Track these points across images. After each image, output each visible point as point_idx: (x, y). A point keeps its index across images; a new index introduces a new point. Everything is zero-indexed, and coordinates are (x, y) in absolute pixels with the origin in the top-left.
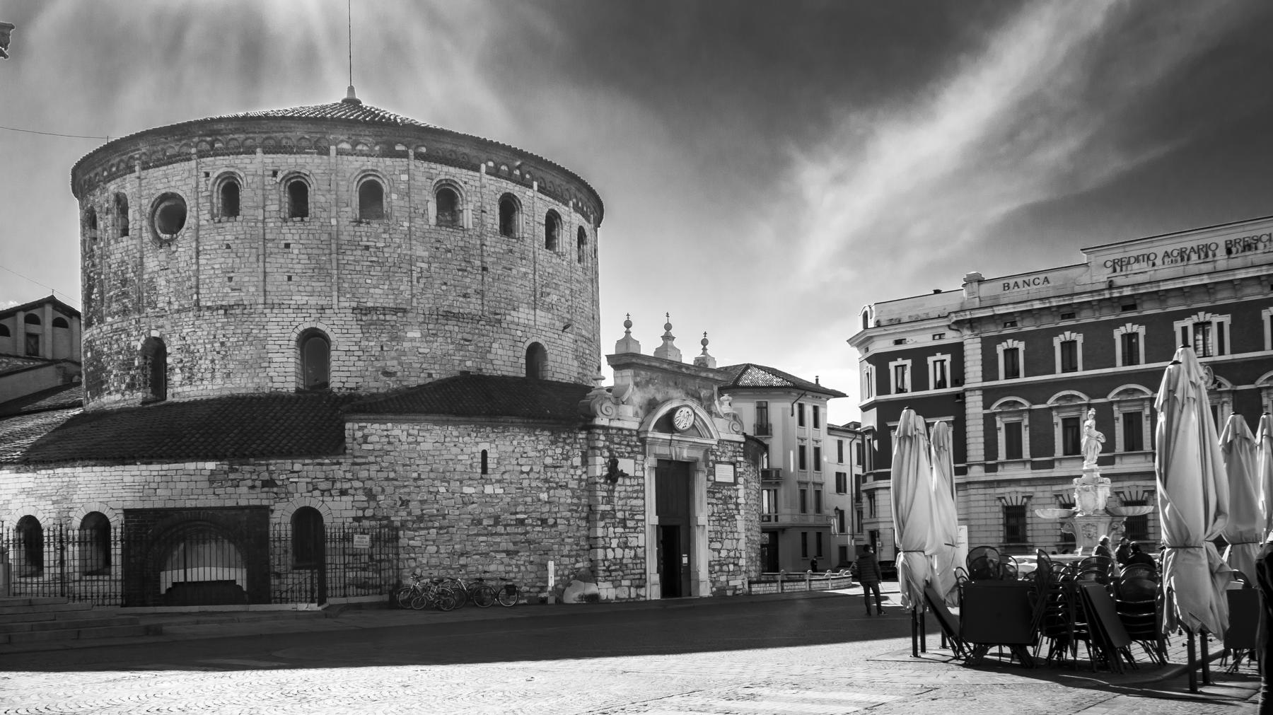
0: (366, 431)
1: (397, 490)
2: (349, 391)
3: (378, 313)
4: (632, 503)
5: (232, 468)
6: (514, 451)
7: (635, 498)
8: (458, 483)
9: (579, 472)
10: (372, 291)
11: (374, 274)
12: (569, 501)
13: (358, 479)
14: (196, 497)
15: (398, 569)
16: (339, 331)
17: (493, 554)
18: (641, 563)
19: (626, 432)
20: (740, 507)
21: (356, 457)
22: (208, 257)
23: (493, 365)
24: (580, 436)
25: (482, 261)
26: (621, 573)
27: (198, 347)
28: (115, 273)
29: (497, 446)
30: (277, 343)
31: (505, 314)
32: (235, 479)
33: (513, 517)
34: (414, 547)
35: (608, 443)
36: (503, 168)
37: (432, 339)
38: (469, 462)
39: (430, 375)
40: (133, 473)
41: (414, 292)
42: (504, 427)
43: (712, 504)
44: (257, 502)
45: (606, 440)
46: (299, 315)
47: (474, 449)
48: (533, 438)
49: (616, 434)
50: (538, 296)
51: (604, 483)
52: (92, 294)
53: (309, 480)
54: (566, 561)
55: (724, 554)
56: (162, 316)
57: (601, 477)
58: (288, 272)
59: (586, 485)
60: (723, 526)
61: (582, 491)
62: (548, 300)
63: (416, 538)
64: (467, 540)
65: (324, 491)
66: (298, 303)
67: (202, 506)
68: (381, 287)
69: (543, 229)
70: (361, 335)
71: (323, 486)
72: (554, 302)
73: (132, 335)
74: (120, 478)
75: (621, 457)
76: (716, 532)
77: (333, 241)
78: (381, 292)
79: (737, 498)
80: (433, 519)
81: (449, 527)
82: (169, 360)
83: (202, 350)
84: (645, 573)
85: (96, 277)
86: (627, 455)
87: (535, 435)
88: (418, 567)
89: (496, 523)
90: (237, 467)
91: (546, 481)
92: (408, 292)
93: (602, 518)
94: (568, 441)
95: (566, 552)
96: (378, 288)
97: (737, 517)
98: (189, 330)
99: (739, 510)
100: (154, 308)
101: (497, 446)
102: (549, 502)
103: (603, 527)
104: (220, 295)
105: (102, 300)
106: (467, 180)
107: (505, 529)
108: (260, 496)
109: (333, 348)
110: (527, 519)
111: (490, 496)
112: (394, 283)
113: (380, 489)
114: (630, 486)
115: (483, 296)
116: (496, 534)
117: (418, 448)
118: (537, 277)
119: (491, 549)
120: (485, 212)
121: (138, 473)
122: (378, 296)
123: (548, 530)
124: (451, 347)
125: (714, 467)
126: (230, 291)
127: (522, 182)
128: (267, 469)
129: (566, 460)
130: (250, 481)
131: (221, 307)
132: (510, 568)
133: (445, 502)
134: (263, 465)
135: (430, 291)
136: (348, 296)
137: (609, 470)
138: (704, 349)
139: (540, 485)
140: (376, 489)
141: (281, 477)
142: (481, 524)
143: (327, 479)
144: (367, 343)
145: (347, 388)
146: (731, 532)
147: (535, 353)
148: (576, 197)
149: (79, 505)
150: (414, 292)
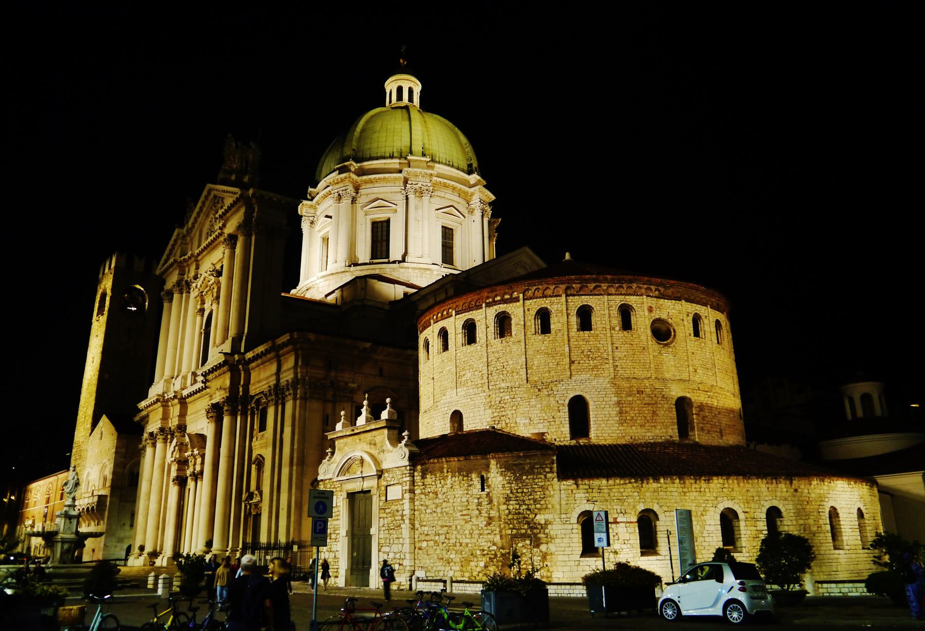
20: (405, 518)
43: (384, 518)
97: (402, 526)
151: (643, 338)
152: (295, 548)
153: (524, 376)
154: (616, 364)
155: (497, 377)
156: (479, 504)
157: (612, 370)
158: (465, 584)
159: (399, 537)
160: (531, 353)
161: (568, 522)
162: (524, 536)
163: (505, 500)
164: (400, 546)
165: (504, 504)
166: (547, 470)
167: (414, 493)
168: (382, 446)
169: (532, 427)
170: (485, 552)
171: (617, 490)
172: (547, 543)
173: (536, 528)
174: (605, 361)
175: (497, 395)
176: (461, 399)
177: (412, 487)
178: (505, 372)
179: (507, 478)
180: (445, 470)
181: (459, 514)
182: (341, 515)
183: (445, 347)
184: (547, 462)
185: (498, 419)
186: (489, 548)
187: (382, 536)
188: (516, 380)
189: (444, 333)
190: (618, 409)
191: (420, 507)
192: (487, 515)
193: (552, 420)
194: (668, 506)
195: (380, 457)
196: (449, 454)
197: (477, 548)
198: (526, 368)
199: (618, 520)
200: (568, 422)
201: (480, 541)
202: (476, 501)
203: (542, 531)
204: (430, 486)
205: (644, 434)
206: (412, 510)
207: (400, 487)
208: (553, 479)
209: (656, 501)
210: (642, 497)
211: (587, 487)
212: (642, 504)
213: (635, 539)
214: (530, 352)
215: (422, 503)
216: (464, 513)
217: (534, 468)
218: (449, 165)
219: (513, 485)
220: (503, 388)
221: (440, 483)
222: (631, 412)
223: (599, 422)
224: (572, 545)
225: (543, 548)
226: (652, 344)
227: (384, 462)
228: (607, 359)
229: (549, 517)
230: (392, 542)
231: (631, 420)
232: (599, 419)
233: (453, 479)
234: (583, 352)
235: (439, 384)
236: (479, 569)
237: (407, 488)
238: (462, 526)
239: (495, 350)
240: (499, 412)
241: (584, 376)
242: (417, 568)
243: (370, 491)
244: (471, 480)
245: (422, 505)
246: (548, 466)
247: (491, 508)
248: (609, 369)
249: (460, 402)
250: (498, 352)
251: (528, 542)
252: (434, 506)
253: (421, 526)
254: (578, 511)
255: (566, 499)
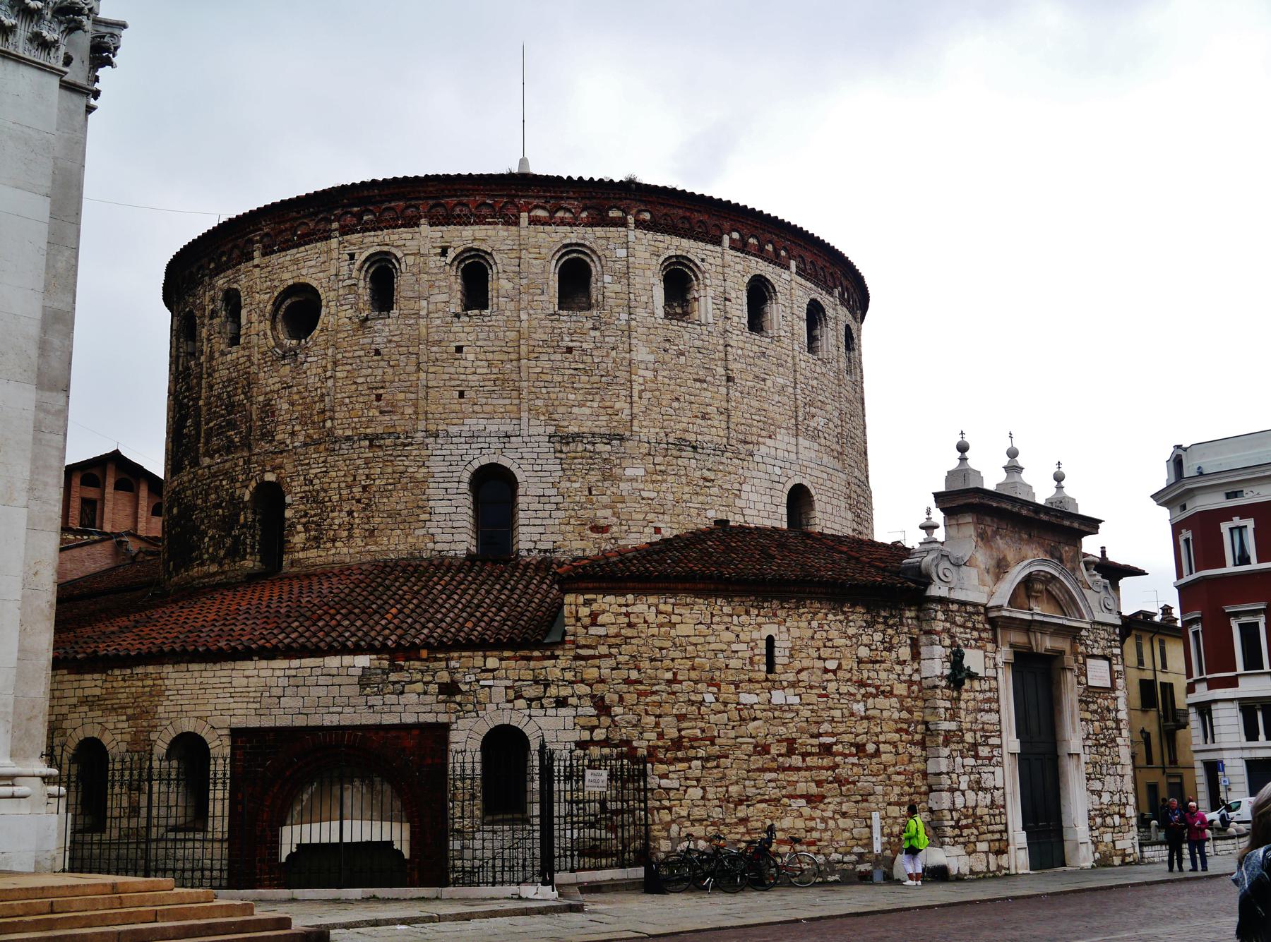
0: (595, 607)
1: (642, 699)
2: (542, 554)
3: (585, 441)
4: (983, 719)
5: (395, 665)
6: (813, 638)
7: (987, 712)
8: (733, 687)
9: (908, 670)
10: (575, 410)
11: (580, 386)
12: (896, 715)
13: (582, 681)
14: (340, 709)
15: (646, 825)
16: (530, 468)
17: (785, 800)
18: (1000, 814)
19: (970, 609)
20: (1122, 726)
21: (579, 647)
22: (348, 367)
23: (744, 515)
24: (908, 614)
25: (726, 369)
26: (975, 832)
27: (331, 493)
28: (219, 396)
29: (788, 630)
30: (441, 485)
31: (758, 443)
32: (398, 682)
33: (815, 741)
34: (668, 790)
35: (948, 625)
36: (751, 240)
37: (660, 478)
38: (748, 654)
39: (657, 530)
40: (246, 673)
41: (635, 411)
42: (798, 602)
43: (1086, 720)
44: (430, 718)
45: (946, 620)
46: (473, 446)
47: (756, 635)
48: (841, 617)
49: (958, 611)
50: (800, 419)
51: (945, 688)
52: (185, 427)
53: (509, 683)
54: (894, 811)
55: (1106, 798)
56: (281, 452)
57: (942, 677)
58: (458, 386)
59: (920, 691)
60: (1102, 755)
61: (915, 699)
62: (813, 424)
63: (671, 775)
64: (748, 779)
65: (531, 700)
66: (472, 429)
67: (348, 723)
68: (589, 404)
69: (804, 325)
70: (561, 473)
71: (530, 692)
72: (820, 428)
73: (238, 481)
74: (228, 680)
75: (966, 646)
76: (1095, 764)
77: (522, 342)
78: (588, 411)
79: (1117, 711)
80: (696, 744)
81: (719, 757)
82: (288, 513)
83: (335, 498)
84: (1006, 831)
85: (191, 403)
86: (973, 642)
87: (844, 613)
88: (673, 821)
89: (791, 752)
90: (402, 663)
91: (861, 684)
92: (627, 412)
93: (947, 742)
94: (891, 622)
95: (893, 798)
96: (584, 406)
97: (1119, 740)
98: (319, 470)
99: (1120, 730)
100: (271, 442)
101: (788, 630)
102: (867, 718)
103: (948, 757)
104: (364, 419)
105: (198, 434)
106: (704, 257)
107: (804, 760)
108: (435, 707)
109: (521, 491)
110: (835, 744)
111: (780, 707)
112: (607, 398)
113: (616, 697)
114: (980, 692)
115: (729, 416)
116: (790, 768)
117: (673, 633)
118: (799, 391)
119: (784, 792)
120: (729, 300)
121: (255, 672)
122: (583, 418)
123: (865, 761)
124: (687, 489)
125: (1085, 664)
126: (377, 414)
127: (775, 260)
128: (447, 666)
129: (889, 650)
130: (420, 684)
131: (366, 437)
132: (812, 824)
133: (713, 718)
134: (440, 660)
135: (657, 409)
136: (542, 418)
137: (952, 667)
138: (1059, 488)
139: (853, 690)
140: (610, 698)
141: (467, 680)
142: (768, 753)
143: (536, 682)
144: (568, 485)
145: (540, 551)
146: (1113, 764)
147: (799, 499)
148: (841, 285)
149: (165, 722)
150: (635, 411)
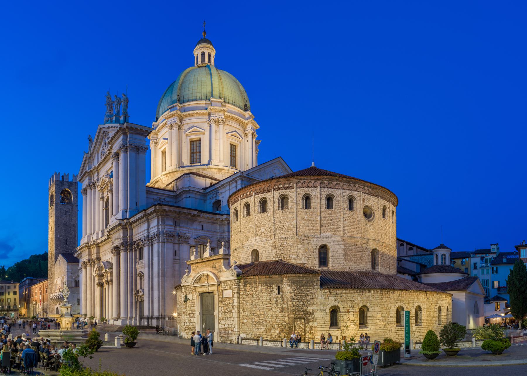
20: (234, 307)
43: (221, 307)
55: (226, 326)
97: (233, 311)
146: (230, 317)
151: (359, 215)
152: (167, 319)
153: (295, 232)
154: (345, 228)
155: (279, 232)
156: (277, 301)
157: (342, 231)
158: (270, 342)
159: (231, 317)
160: (299, 219)
161: (325, 311)
162: (301, 318)
163: (291, 299)
164: (232, 321)
165: (291, 301)
166: (315, 284)
167: (239, 294)
168: (220, 268)
169: (298, 260)
170: (279, 326)
171: (350, 296)
172: (313, 322)
173: (308, 314)
174: (339, 227)
175: (279, 241)
176: (258, 243)
177: (238, 291)
178: (284, 229)
179: (293, 288)
180: (258, 283)
181: (265, 306)
182: (196, 304)
183: (248, 214)
184: (315, 280)
185: (279, 255)
186: (281, 323)
187: (220, 316)
188: (290, 234)
189: (247, 206)
190: (344, 253)
191: (243, 302)
192: (281, 307)
193: (309, 257)
194: (374, 305)
195: (219, 274)
196: (260, 274)
197: (275, 323)
198: (296, 227)
199: (350, 311)
200: (318, 258)
201: (277, 320)
202: (275, 299)
203: (311, 315)
204: (248, 291)
205: (356, 267)
206: (238, 303)
207: (231, 291)
208: (318, 289)
209: (369, 302)
210: (362, 300)
211: (335, 294)
212: (362, 303)
213: (357, 321)
214: (299, 219)
215: (244, 299)
216: (268, 305)
217: (308, 283)
218: (234, 105)
219: (296, 292)
220: (283, 238)
221: (255, 289)
222: (351, 255)
223: (334, 259)
224: (326, 322)
225: (311, 324)
226: (363, 218)
227: (221, 277)
228: (340, 225)
229: (315, 308)
230: (226, 319)
231: (350, 259)
232: (334, 257)
233: (262, 287)
234: (328, 221)
235: (245, 234)
236: (275, 334)
237: (236, 291)
238: (267, 312)
239: (278, 216)
240: (280, 251)
241: (327, 234)
242: (241, 333)
243: (213, 292)
244: (272, 288)
245: (244, 301)
246: (315, 282)
247: (283, 303)
248: (340, 232)
249: (257, 245)
250: (280, 218)
251: (303, 321)
252: (251, 301)
253: (243, 312)
254: (330, 306)
255: (324, 299)
